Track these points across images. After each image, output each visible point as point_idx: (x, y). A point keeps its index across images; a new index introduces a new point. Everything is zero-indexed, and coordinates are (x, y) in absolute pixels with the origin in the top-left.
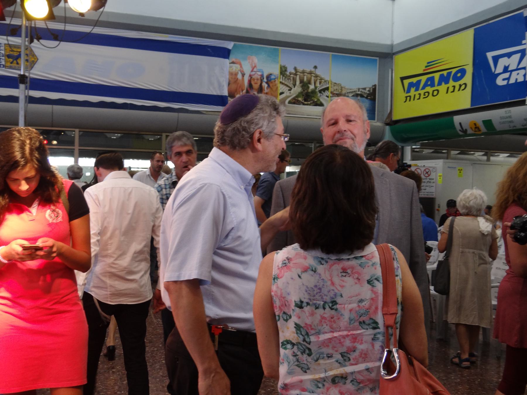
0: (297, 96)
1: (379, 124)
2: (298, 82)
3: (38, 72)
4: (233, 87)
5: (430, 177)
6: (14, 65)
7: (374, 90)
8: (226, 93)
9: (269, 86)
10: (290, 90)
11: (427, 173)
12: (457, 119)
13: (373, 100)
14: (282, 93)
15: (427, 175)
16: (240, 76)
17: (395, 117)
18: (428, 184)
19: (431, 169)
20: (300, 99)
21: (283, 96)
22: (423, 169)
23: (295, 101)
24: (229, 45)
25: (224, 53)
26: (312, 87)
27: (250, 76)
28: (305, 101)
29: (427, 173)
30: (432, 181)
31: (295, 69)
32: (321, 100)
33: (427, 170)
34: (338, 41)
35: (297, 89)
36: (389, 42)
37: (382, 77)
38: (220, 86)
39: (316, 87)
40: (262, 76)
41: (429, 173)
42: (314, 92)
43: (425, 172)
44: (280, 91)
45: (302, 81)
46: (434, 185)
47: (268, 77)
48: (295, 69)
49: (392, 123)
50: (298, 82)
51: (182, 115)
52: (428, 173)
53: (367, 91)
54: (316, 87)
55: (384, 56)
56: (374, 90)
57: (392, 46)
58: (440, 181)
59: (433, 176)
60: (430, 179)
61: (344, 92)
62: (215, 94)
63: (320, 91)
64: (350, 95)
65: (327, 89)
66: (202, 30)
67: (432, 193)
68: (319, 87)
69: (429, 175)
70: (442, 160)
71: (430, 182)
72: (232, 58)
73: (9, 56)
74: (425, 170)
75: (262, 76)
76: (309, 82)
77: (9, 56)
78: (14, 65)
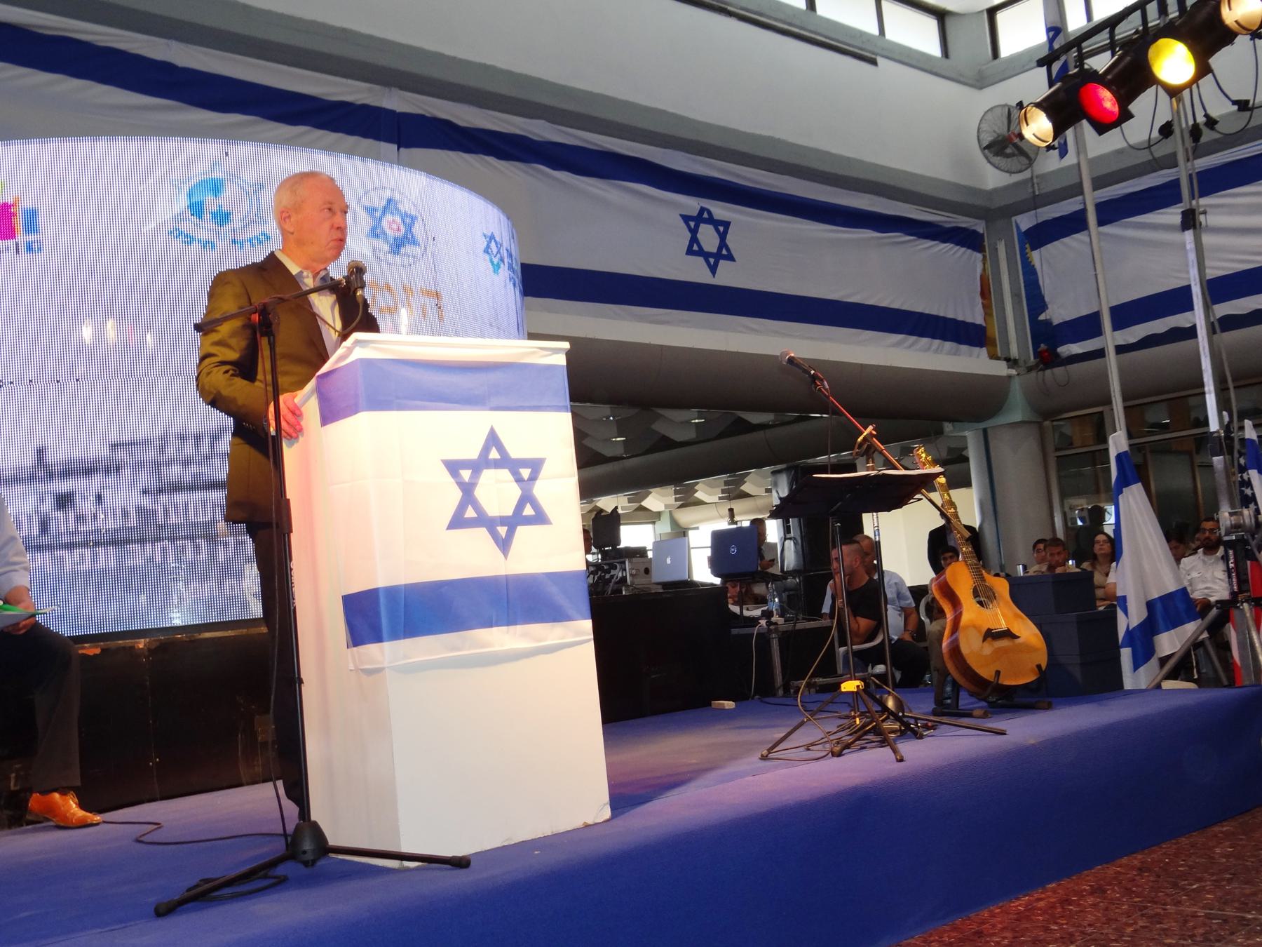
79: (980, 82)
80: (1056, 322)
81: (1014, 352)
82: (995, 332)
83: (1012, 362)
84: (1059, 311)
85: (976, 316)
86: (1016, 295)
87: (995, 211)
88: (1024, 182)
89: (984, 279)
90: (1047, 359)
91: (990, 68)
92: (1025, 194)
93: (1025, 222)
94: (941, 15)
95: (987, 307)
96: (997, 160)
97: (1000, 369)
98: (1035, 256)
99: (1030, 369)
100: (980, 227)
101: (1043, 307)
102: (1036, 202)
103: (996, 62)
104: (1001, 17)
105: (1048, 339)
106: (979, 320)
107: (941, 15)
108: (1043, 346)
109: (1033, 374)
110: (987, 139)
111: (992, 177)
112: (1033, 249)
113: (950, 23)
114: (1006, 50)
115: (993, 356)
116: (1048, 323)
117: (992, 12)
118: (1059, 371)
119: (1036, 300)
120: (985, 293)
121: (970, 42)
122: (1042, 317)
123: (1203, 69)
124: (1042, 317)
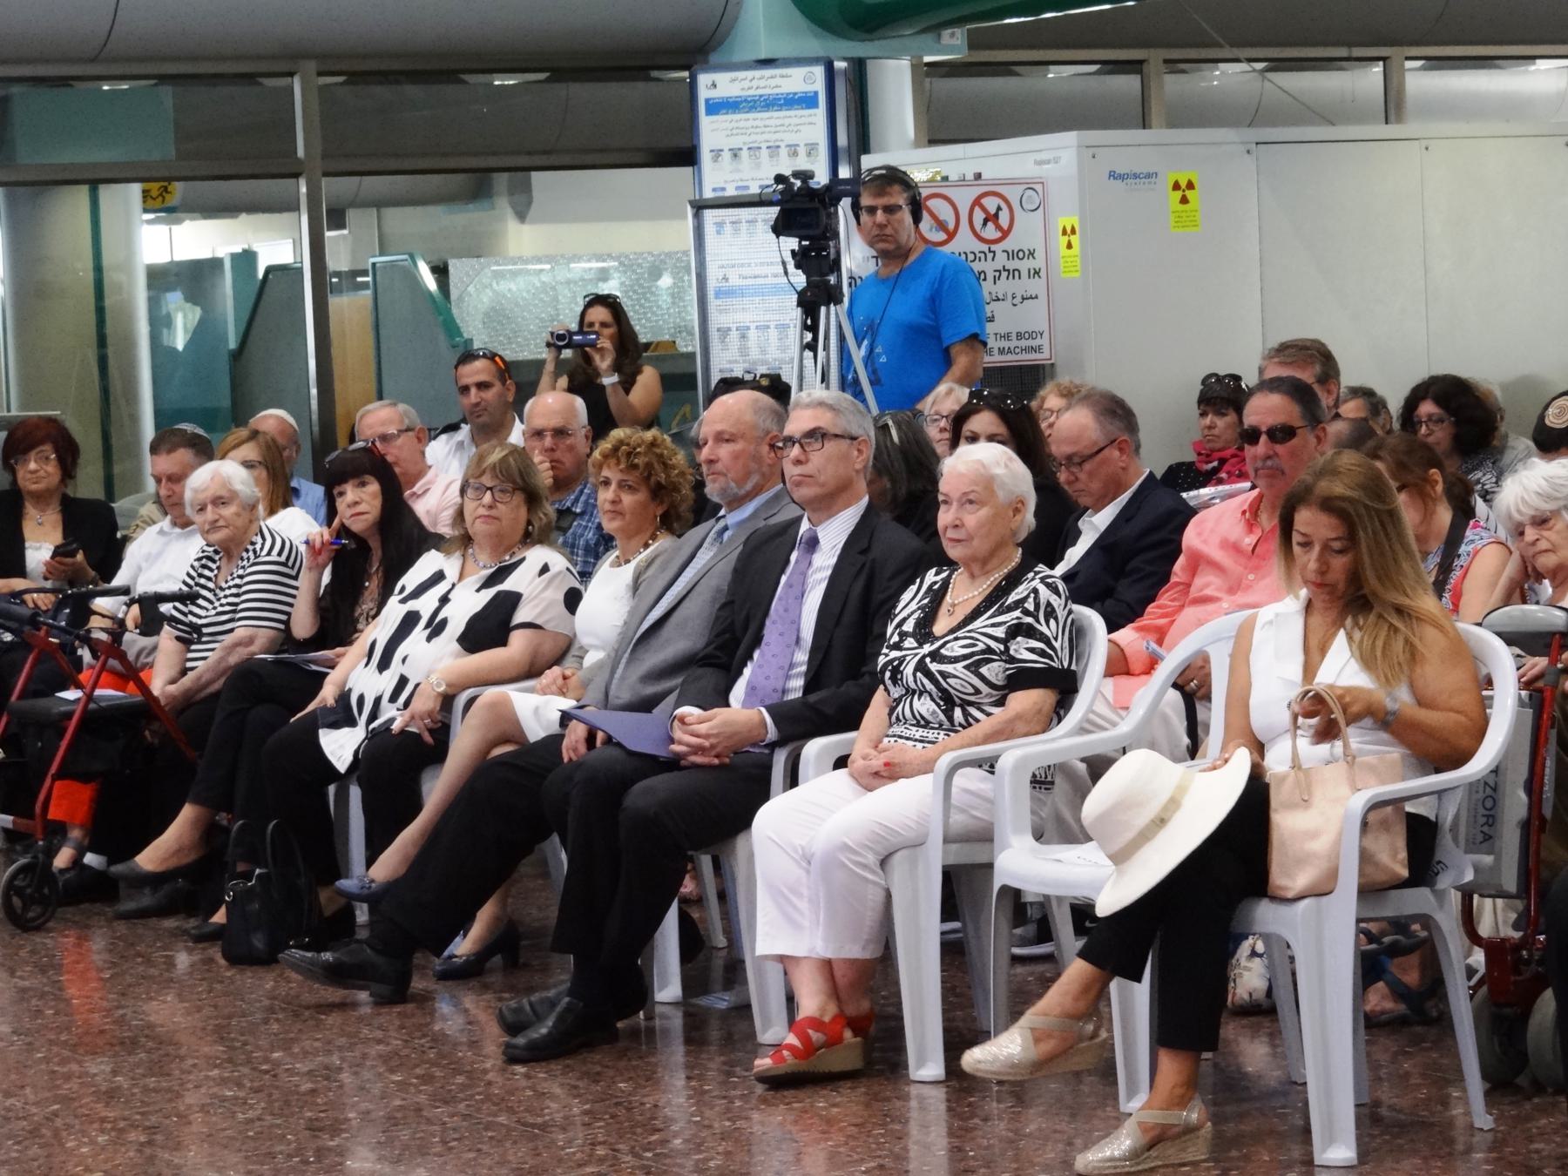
5: (1009, 244)
11: (991, 218)
15: (991, 232)
18: (1004, 286)
19: (1013, 194)
22: (964, 198)
29: (991, 218)
30: (1024, 265)
33: (991, 204)
41: (1004, 219)
43: (979, 216)
46: (1037, 286)
52: (993, 215)
58: (1069, 260)
59: (1028, 231)
60: (1011, 255)
67: (1031, 335)
69: (1006, 234)
70: (1070, 138)
71: (1013, 273)
74: (977, 202)
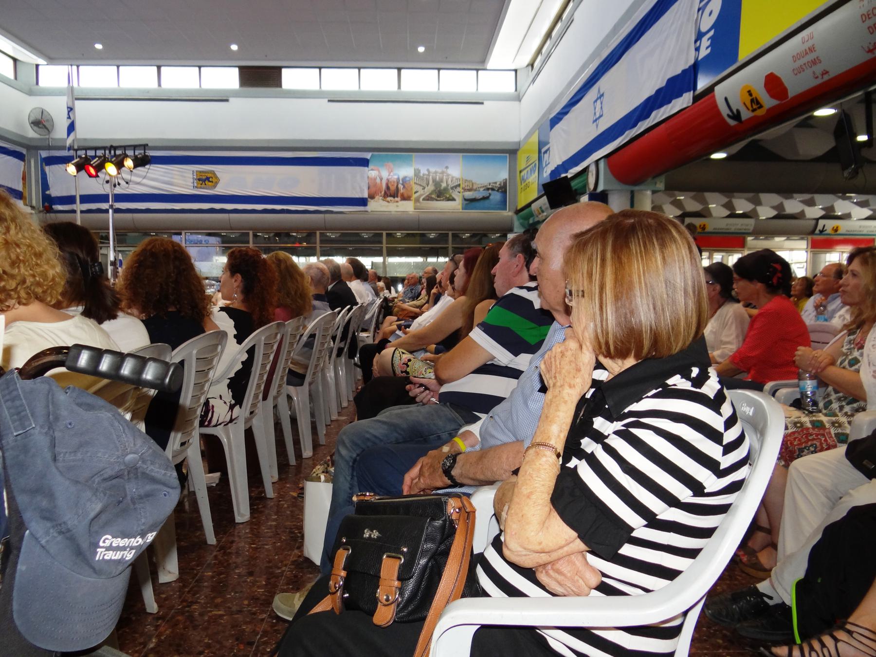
0: (431, 194)
1: (510, 214)
2: (431, 182)
3: (220, 190)
4: (373, 190)
6: (203, 185)
7: (505, 184)
8: (366, 195)
9: (404, 187)
10: (424, 188)
12: (533, 205)
13: (505, 192)
14: (416, 192)
16: (378, 181)
17: (519, 208)
20: (433, 196)
21: (417, 194)
23: (429, 198)
24: (368, 155)
25: (364, 163)
26: (444, 185)
27: (388, 180)
28: (438, 196)
31: (428, 170)
32: (454, 196)
34: (465, 143)
35: (431, 188)
36: (516, 139)
37: (512, 171)
38: (362, 191)
39: (448, 185)
40: (398, 178)
42: (446, 189)
44: (414, 191)
45: (434, 181)
47: (404, 179)
48: (428, 170)
49: (517, 212)
50: (431, 182)
51: (327, 216)
53: (498, 185)
54: (448, 185)
55: (511, 152)
56: (505, 184)
57: (519, 143)
61: (475, 187)
62: (357, 196)
63: (452, 188)
64: (482, 189)
65: (459, 185)
66: (343, 146)
68: (451, 185)
72: (371, 166)
73: (199, 180)
75: (398, 178)
76: (442, 181)
77: (199, 180)
78: (203, 185)
79: (30, 93)
80: (53, 195)
81: (34, 203)
82: (26, 194)
83: (33, 207)
84: (55, 191)
85: (20, 188)
86: (37, 181)
87: (33, 147)
88: (46, 139)
89: (24, 173)
90: (48, 209)
91: (33, 90)
92: (45, 144)
93: (44, 154)
94: (15, 60)
95: (24, 184)
96: (35, 128)
97: (28, 210)
98: (47, 169)
99: (40, 212)
100: (24, 151)
101: (48, 189)
102: (49, 148)
103: (36, 87)
104: (40, 67)
105: (49, 202)
106: (21, 189)
107: (15, 60)
108: (46, 204)
109: (41, 214)
110: (32, 119)
111: (31, 133)
112: (47, 165)
113: (18, 63)
114: (43, 83)
115: (25, 204)
116: (49, 196)
117: (37, 66)
118: (52, 215)
119: (45, 186)
120: (24, 179)
121: (27, 75)
122: (47, 192)
123: (119, 173)
124: (47, 192)
